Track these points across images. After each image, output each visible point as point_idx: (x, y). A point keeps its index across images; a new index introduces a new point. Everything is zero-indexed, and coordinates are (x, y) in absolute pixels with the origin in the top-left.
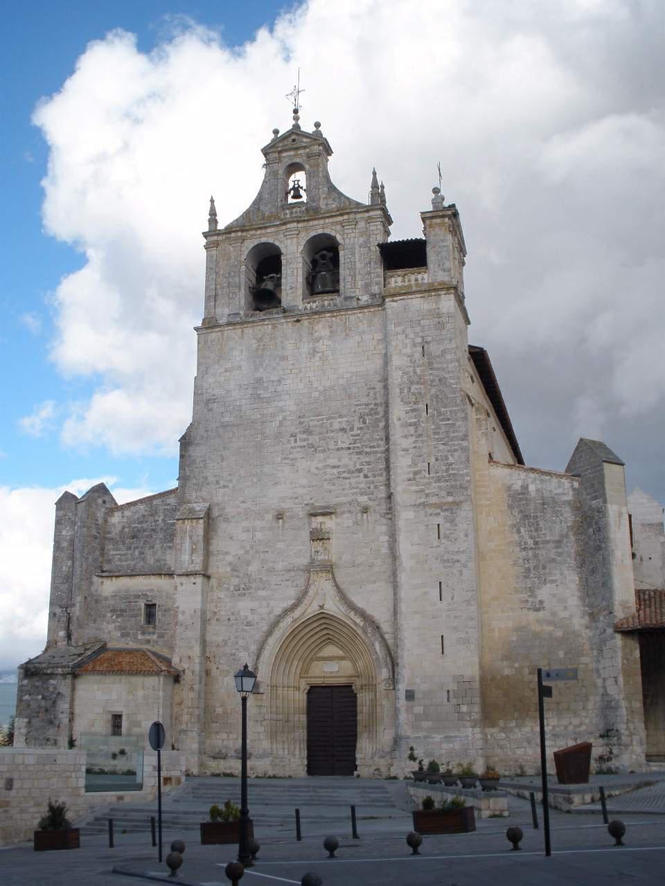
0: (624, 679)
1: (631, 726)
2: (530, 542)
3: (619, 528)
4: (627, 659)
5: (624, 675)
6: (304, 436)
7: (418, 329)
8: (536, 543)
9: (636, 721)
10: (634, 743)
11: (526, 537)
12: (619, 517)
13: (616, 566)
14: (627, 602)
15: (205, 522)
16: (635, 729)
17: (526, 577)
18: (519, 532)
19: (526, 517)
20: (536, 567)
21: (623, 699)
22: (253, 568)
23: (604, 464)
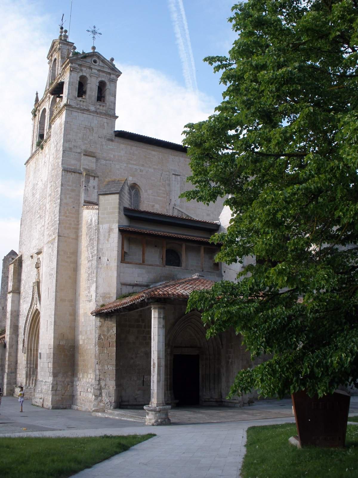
0: (98, 349)
1: (103, 383)
2: (91, 256)
3: (108, 240)
4: (104, 335)
5: (99, 347)
6: (39, 211)
7: (56, 137)
8: (92, 257)
9: (108, 379)
10: (104, 395)
11: (90, 253)
12: (109, 232)
13: (101, 268)
14: (109, 294)
15: (15, 265)
16: (105, 385)
17: (88, 280)
18: (88, 251)
19: (90, 239)
20: (91, 272)
21: (97, 364)
22: (27, 286)
23: (101, 197)
